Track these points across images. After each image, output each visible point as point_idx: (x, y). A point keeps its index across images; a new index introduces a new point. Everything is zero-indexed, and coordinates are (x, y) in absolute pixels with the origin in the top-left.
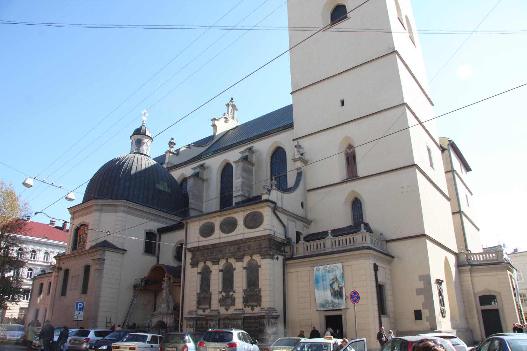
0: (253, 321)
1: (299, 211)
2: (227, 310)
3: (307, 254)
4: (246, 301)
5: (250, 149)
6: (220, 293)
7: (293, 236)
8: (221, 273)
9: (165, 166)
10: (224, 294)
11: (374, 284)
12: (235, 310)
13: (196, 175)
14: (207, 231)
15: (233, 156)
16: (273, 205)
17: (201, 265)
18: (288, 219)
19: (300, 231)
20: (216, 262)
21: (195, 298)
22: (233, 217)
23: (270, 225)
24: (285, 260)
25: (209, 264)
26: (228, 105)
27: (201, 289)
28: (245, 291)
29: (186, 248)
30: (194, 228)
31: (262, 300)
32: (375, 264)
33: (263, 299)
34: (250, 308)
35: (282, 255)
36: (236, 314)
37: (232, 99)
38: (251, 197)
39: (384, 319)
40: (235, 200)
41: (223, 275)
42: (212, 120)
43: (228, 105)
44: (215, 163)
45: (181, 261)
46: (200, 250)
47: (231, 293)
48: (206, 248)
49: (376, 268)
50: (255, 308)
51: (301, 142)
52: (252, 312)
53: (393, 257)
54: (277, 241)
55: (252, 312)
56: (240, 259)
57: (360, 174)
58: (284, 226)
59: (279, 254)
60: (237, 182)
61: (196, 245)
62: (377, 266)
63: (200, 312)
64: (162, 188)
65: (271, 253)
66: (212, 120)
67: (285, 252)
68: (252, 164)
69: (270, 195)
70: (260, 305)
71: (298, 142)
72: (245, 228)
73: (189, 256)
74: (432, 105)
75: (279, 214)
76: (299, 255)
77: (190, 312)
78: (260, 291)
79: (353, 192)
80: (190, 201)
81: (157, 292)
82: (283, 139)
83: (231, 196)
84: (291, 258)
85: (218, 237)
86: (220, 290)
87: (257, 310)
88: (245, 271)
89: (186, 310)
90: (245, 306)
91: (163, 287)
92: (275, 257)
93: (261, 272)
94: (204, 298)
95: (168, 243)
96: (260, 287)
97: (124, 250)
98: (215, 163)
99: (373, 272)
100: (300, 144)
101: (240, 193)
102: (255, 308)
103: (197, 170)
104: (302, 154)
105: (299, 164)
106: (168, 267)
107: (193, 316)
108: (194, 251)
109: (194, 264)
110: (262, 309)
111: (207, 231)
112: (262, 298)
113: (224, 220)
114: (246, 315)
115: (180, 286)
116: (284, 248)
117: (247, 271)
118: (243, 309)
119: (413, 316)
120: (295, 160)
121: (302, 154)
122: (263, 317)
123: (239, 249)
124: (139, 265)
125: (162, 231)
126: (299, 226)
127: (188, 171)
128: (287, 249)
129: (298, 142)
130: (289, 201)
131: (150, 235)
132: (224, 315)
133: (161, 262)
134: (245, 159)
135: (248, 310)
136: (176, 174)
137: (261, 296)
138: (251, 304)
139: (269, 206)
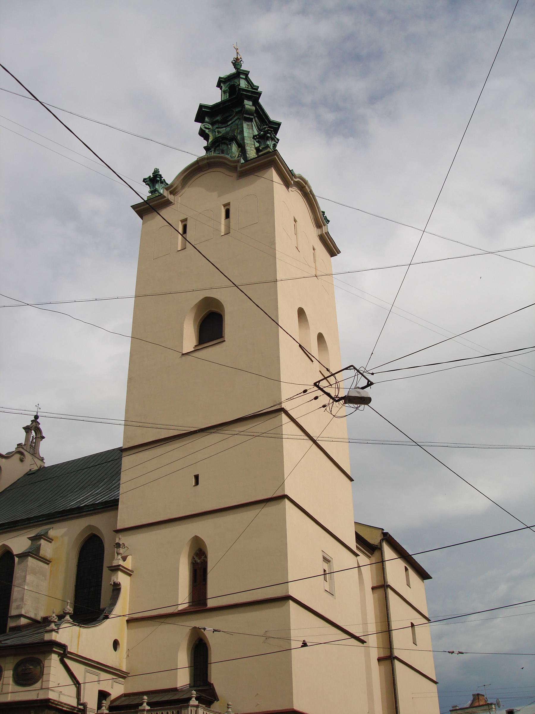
7: (91, 699)
26: (27, 429)
37: (36, 417)
38: (39, 618)
43: (27, 429)
58: (77, 683)
74: (351, 480)
121: (124, 559)
139: (56, 652)
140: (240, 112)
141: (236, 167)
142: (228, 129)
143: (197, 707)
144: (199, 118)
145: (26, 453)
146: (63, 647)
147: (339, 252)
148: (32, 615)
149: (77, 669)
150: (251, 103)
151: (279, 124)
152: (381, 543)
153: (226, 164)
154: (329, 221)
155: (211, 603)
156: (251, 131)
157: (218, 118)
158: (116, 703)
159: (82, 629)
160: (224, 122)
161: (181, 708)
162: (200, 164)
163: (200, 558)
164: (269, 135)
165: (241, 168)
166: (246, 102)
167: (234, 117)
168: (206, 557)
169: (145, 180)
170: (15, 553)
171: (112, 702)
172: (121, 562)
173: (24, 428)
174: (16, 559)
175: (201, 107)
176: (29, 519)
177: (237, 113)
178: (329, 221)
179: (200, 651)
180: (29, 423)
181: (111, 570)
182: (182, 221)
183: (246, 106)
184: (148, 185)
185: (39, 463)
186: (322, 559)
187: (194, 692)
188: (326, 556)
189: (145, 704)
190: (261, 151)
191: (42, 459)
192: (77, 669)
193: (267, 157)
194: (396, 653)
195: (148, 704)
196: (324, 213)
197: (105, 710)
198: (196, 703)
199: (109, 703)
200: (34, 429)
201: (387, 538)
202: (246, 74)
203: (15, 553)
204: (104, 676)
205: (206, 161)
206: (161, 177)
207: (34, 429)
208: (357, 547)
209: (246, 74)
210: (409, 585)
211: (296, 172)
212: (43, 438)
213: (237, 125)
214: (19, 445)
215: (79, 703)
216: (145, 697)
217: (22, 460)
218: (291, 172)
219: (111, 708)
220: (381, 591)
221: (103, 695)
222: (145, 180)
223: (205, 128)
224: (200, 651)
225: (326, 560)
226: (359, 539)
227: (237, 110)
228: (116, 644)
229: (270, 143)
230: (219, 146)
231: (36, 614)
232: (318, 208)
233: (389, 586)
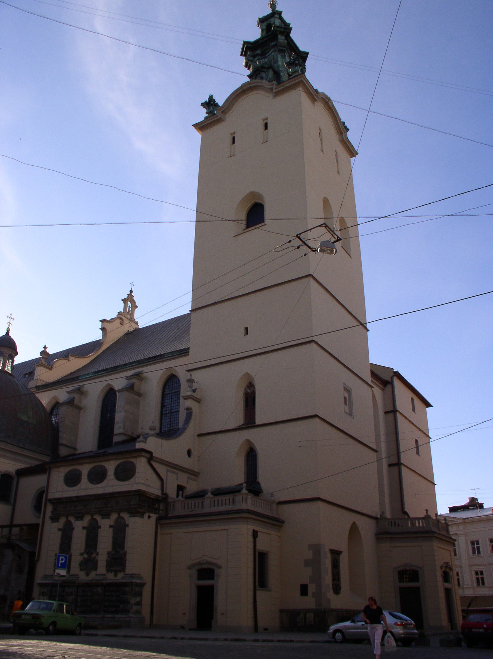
1: (184, 461)
2: (87, 575)
5: (138, 376)
6: (82, 554)
7: (171, 491)
8: (85, 531)
9: (32, 384)
10: (86, 556)
11: (251, 551)
12: (97, 575)
13: (70, 403)
14: (72, 480)
15: (118, 381)
16: (148, 455)
17: (63, 520)
19: (183, 483)
20: (80, 517)
22: (103, 466)
23: (144, 479)
24: (158, 519)
26: (125, 301)
27: (61, 548)
28: (109, 553)
30: (58, 475)
31: (127, 565)
32: (254, 531)
33: (128, 563)
34: (113, 573)
35: (155, 513)
37: (131, 292)
38: (135, 436)
39: (261, 594)
40: (116, 439)
43: (125, 301)
45: (40, 512)
47: (93, 556)
48: (69, 500)
49: (255, 534)
51: (197, 376)
53: (283, 522)
54: (150, 498)
56: (106, 515)
59: (152, 512)
60: (119, 416)
61: (58, 495)
62: (257, 532)
64: (25, 418)
65: (141, 510)
67: (160, 510)
68: (139, 395)
69: (145, 443)
70: (124, 570)
71: (191, 376)
72: (115, 479)
73: (50, 508)
75: (155, 465)
76: (176, 514)
77: (46, 577)
78: (125, 554)
79: (248, 441)
80: (61, 434)
84: (166, 517)
85: (85, 488)
86: (83, 551)
87: (120, 575)
88: (111, 529)
90: (109, 570)
92: (146, 515)
96: (125, 549)
98: (95, 389)
99: (251, 539)
100: (192, 378)
101: (121, 431)
103: (72, 395)
104: (194, 391)
105: (189, 403)
107: (47, 582)
108: (57, 502)
109: (55, 519)
110: (125, 574)
111: (72, 480)
112: (127, 561)
113: (94, 468)
114: (107, 581)
117: (113, 531)
118: (105, 575)
119: (298, 591)
120: (186, 398)
121: (194, 391)
122: (125, 584)
123: (107, 503)
125: (21, 473)
126: (183, 479)
127: (62, 394)
128: (162, 506)
129: (191, 376)
134: (130, 388)
136: (45, 399)
139: (144, 456)
140: (275, 45)
141: (272, 89)
142: (266, 60)
143: (246, 494)
144: (244, 53)
145: (124, 318)
146: (150, 453)
147: (357, 154)
148: (131, 434)
149: (161, 469)
150: (283, 38)
151: (307, 54)
152: (392, 378)
153: (263, 86)
154: (349, 130)
155: (258, 422)
156: (284, 60)
157: (259, 52)
159: (163, 441)
160: (263, 55)
162: (244, 88)
163: (250, 389)
164: (297, 62)
165: (275, 89)
166: (279, 37)
167: (271, 50)
168: (254, 388)
169: (202, 104)
170: (116, 388)
172: (192, 394)
173: (122, 300)
174: (117, 393)
175: (245, 43)
176: (125, 365)
177: (273, 46)
178: (349, 130)
180: (126, 296)
181: (185, 399)
182: (232, 134)
183: (279, 40)
184: (204, 107)
185: (135, 326)
186: (342, 389)
188: (346, 387)
190: (291, 75)
191: (137, 323)
192: (161, 469)
193: (296, 80)
194: (402, 462)
196: (344, 123)
198: (247, 492)
200: (129, 299)
201: (397, 375)
202: (280, 13)
204: (181, 475)
205: (248, 86)
206: (214, 101)
207: (129, 300)
208: (372, 380)
209: (280, 13)
210: (414, 410)
211: (320, 91)
212: (137, 307)
213: (273, 56)
214: (119, 313)
215: (163, 493)
217: (121, 324)
218: (316, 91)
220: (391, 415)
221: (180, 488)
222: (202, 104)
223: (249, 60)
224: (251, 456)
225: (347, 390)
226: (374, 374)
227: (273, 44)
228: (189, 453)
229: (298, 68)
230: (259, 74)
232: (340, 119)
233: (397, 411)
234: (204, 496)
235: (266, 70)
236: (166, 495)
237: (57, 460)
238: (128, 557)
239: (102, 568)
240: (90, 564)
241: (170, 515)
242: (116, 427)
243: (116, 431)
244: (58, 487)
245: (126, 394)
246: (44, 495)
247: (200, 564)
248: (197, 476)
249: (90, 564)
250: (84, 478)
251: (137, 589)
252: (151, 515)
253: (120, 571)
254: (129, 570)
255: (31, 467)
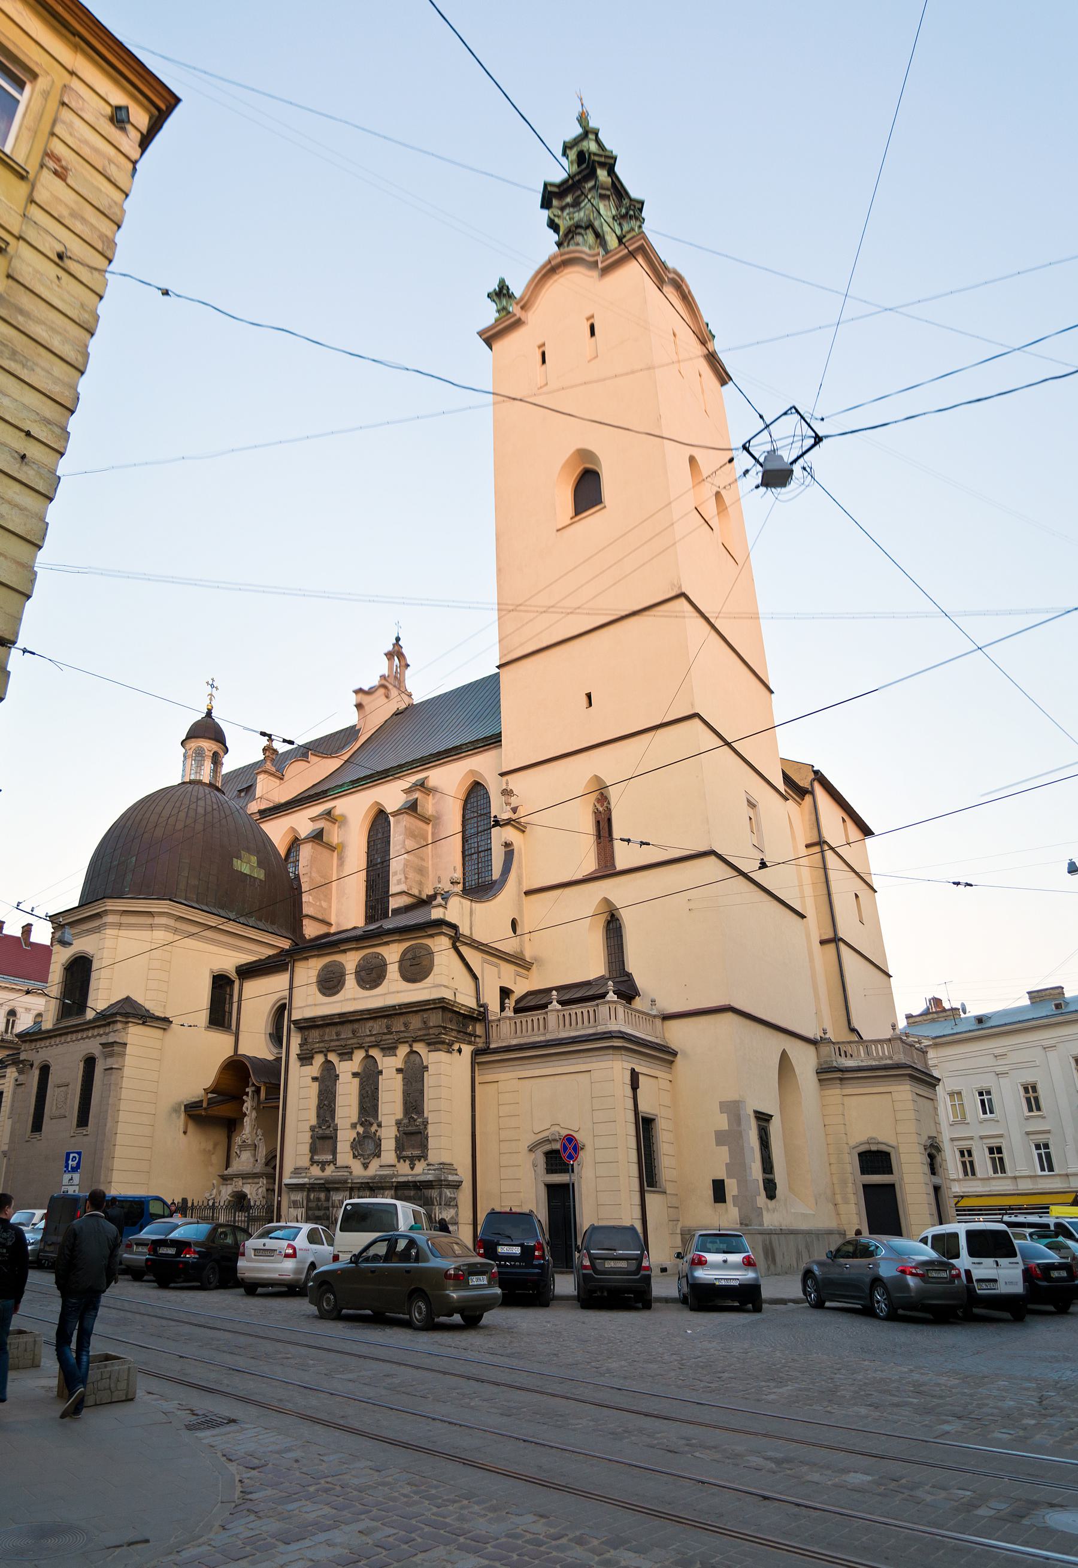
0: (412, 1193)
3: (514, 1042)
4: (400, 1147)
5: (422, 785)
8: (357, 1080)
15: (391, 795)
17: (319, 1060)
18: (484, 961)
20: (346, 1054)
21: (306, 1138)
25: (332, 1057)
28: (398, 1123)
29: (289, 1020)
34: (408, 1162)
35: (470, 1043)
36: (380, 1176)
37: (398, 639)
41: (361, 1084)
42: (356, 692)
44: (355, 809)
46: (318, 1026)
50: (416, 1162)
52: (410, 1172)
55: (410, 1172)
56: (390, 1050)
57: (620, 865)
61: (309, 1013)
63: (316, 1171)
66: (356, 692)
67: (476, 1036)
70: (425, 1157)
73: (296, 1040)
81: (232, 1125)
82: (482, 764)
83: (386, 895)
87: (420, 1167)
89: (288, 1167)
90: (399, 1158)
91: (244, 1109)
93: (429, 1080)
94: (323, 1138)
95: (258, 998)
97: (167, 1021)
102: (416, 1162)
106: (254, 1060)
108: (307, 1026)
115: (278, 1107)
116: (474, 1029)
124: (196, 1057)
130: (484, 920)
131: (221, 984)
132: (359, 1177)
133: (241, 1051)
134: (412, 808)
135: (404, 1168)
137: (427, 1138)
138: (408, 1153)
158: (521, 1005)
161: (597, 1005)
171: (517, 1002)
174: (391, 819)
179: (613, 927)
180: (391, 648)
187: (610, 983)
189: (555, 1003)
195: (559, 1002)
197: (509, 1013)
199: (513, 1004)
200: (396, 653)
203: (389, 811)
207: (396, 653)
214: (383, 677)
216: (554, 993)
219: (517, 1011)
221: (505, 993)
224: (613, 927)
231: (420, 892)
234: (544, 1006)
235: (583, 231)
236: (484, 1006)
237: (303, 949)
238: (431, 1130)
239: (389, 1154)
240: (366, 1145)
241: (492, 1046)
242: (393, 880)
243: (393, 889)
244: (310, 1003)
245: (406, 820)
246: (286, 1012)
247: (548, 1141)
248: (528, 969)
249: (366, 1145)
250: (350, 981)
251: (448, 1193)
252: (463, 1046)
253: (419, 1158)
254: (433, 1156)
255: (260, 960)
